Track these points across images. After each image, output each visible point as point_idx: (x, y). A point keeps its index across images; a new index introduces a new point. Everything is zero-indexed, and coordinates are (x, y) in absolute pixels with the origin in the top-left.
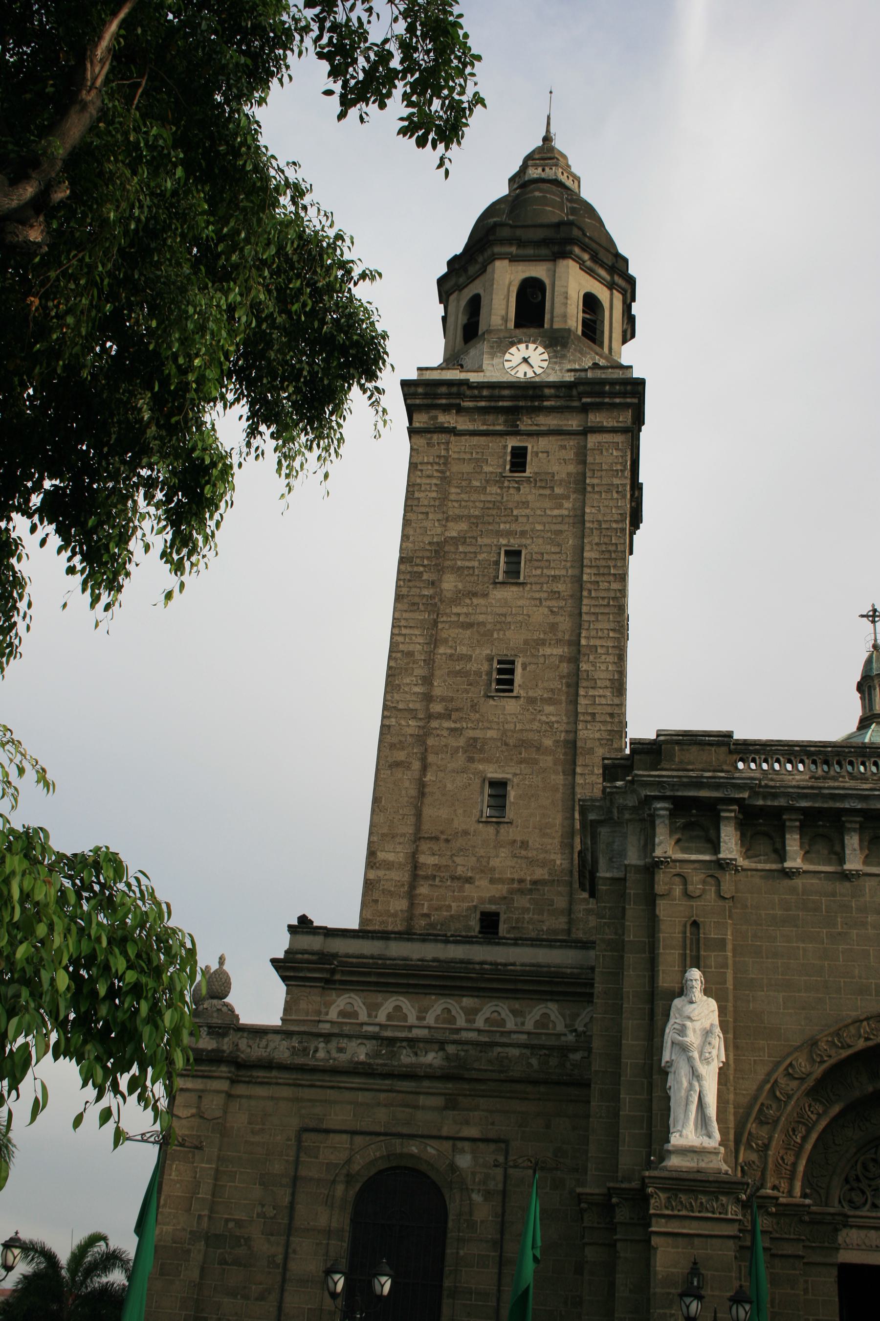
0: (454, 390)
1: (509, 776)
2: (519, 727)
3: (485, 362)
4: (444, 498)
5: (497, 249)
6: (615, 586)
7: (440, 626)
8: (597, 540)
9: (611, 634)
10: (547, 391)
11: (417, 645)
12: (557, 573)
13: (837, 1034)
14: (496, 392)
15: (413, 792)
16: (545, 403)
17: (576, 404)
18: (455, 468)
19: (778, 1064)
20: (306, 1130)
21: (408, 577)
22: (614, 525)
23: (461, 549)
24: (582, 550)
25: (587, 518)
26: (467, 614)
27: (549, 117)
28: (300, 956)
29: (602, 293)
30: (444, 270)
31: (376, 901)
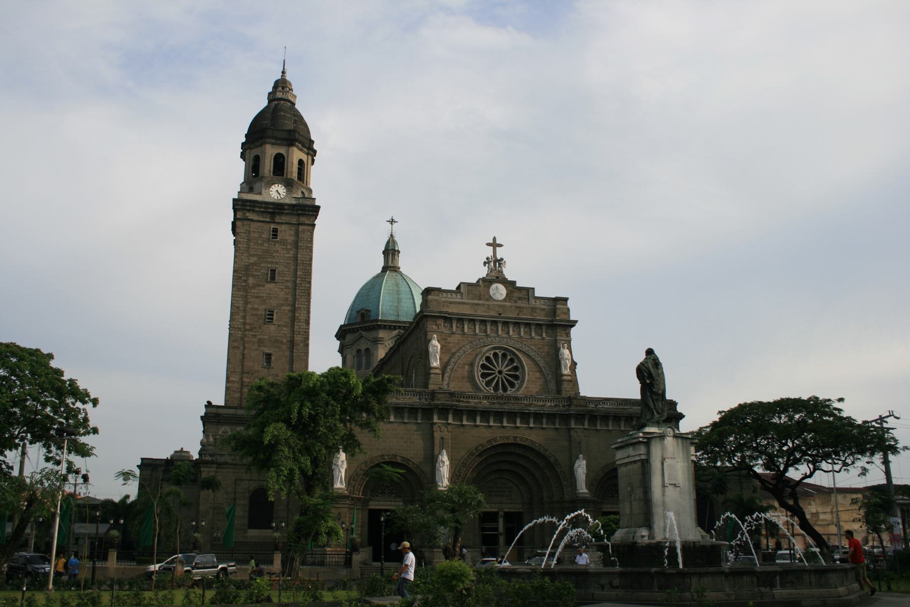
0: (252, 204)
1: (272, 352)
2: (275, 335)
3: (263, 191)
4: (249, 248)
5: (267, 140)
6: (307, 285)
7: (248, 297)
8: (301, 267)
9: (306, 303)
10: (286, 207)
11: (240, 304)
12: (288, 279)
13: (372, 460)
14: (268, 206)
15: (241, 357)
16: (285, 212)
17: (295, 213)
18: (252, 235)
19: (358, 467)
20: (237, 480)
21: (236, 278)
22: (308, 262)
23: (255, 268)
24: (297, 271)
25: (299, 259)
26: (257, 293)
27: (284, 61)
28: (209, 415)
29: (305, 159)
30: (244, 140)
31: (230, 394)
